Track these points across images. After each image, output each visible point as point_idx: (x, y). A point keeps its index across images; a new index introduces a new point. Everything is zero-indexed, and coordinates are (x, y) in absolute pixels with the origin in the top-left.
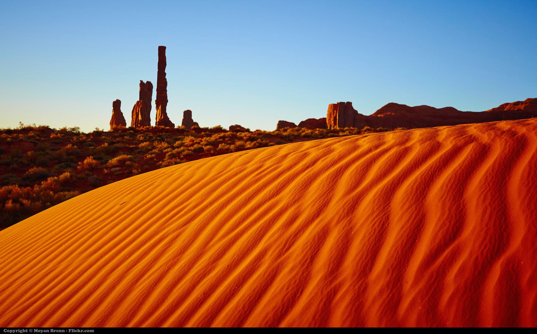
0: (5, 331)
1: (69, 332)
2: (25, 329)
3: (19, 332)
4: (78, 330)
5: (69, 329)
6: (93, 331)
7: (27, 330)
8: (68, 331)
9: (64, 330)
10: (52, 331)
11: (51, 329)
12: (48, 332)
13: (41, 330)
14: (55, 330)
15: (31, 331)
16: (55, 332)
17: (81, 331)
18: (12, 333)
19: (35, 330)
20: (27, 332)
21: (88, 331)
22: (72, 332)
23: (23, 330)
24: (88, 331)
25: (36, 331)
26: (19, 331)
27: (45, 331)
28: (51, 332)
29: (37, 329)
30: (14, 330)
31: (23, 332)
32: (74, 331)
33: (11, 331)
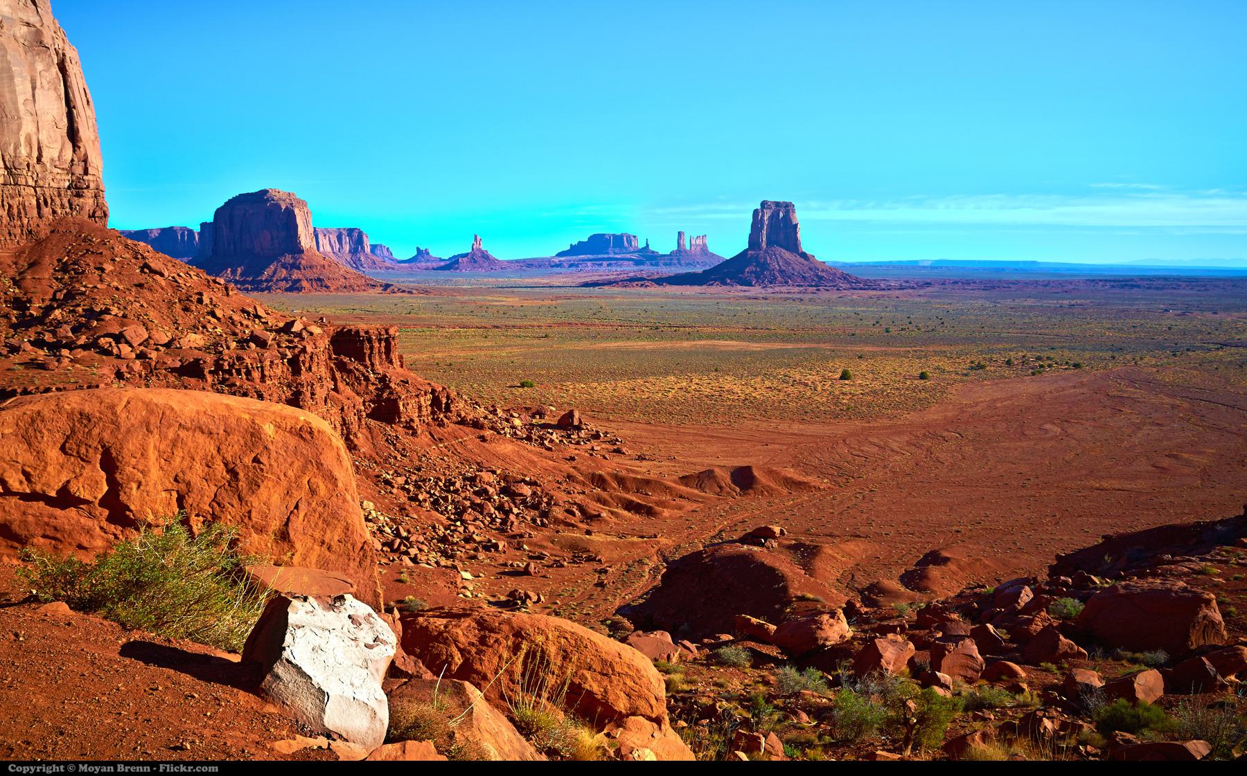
0: (13, 768)
1: (161, 770)
2: (58, 764)
3: (44, 771)
4: (181, 766)
5: (161, 765)
6: (215, 769)
7: (62, 767)
8: (159, 768)
9: (148, 768)
10: (121, 768)
11: (119, 765)
12: (112, 771)
13: (96, 767)
14: (126, 767)
15: (71, 768)
16: (127, 771)
17: (187, 769)
18: (28, 773)
19: (81, 766)
20: (62, 770)
21: (205, 769)
22: (168, 771)
23: (54, 766)
24: (205, 769)
25: (83, 768)
26: (44, 768)
27: (104, 769)
28: (119, 770)
29: (86, 765)
30: (31, 767)
31: (54, 771)
32: (171, 769)
33: (25, 770)
